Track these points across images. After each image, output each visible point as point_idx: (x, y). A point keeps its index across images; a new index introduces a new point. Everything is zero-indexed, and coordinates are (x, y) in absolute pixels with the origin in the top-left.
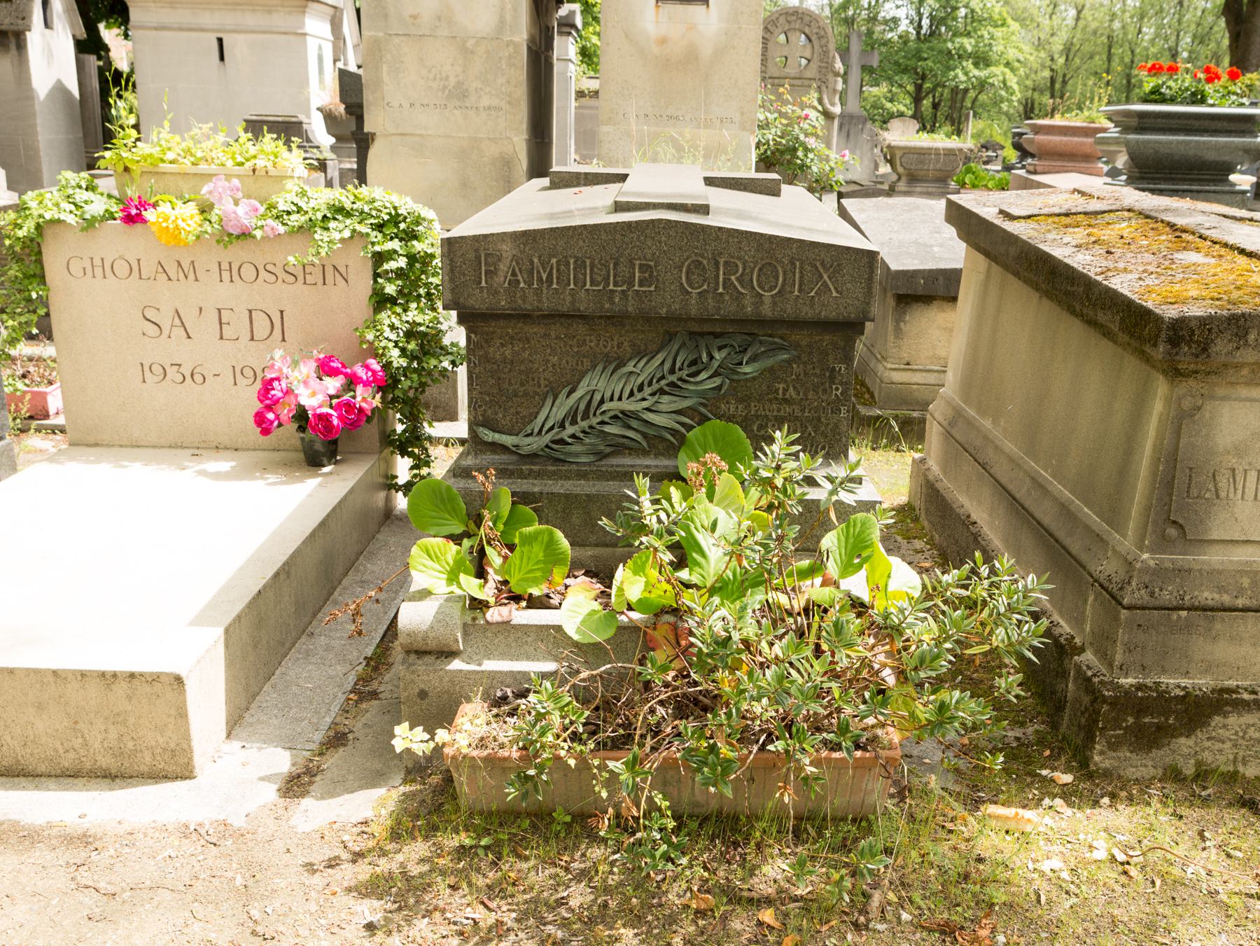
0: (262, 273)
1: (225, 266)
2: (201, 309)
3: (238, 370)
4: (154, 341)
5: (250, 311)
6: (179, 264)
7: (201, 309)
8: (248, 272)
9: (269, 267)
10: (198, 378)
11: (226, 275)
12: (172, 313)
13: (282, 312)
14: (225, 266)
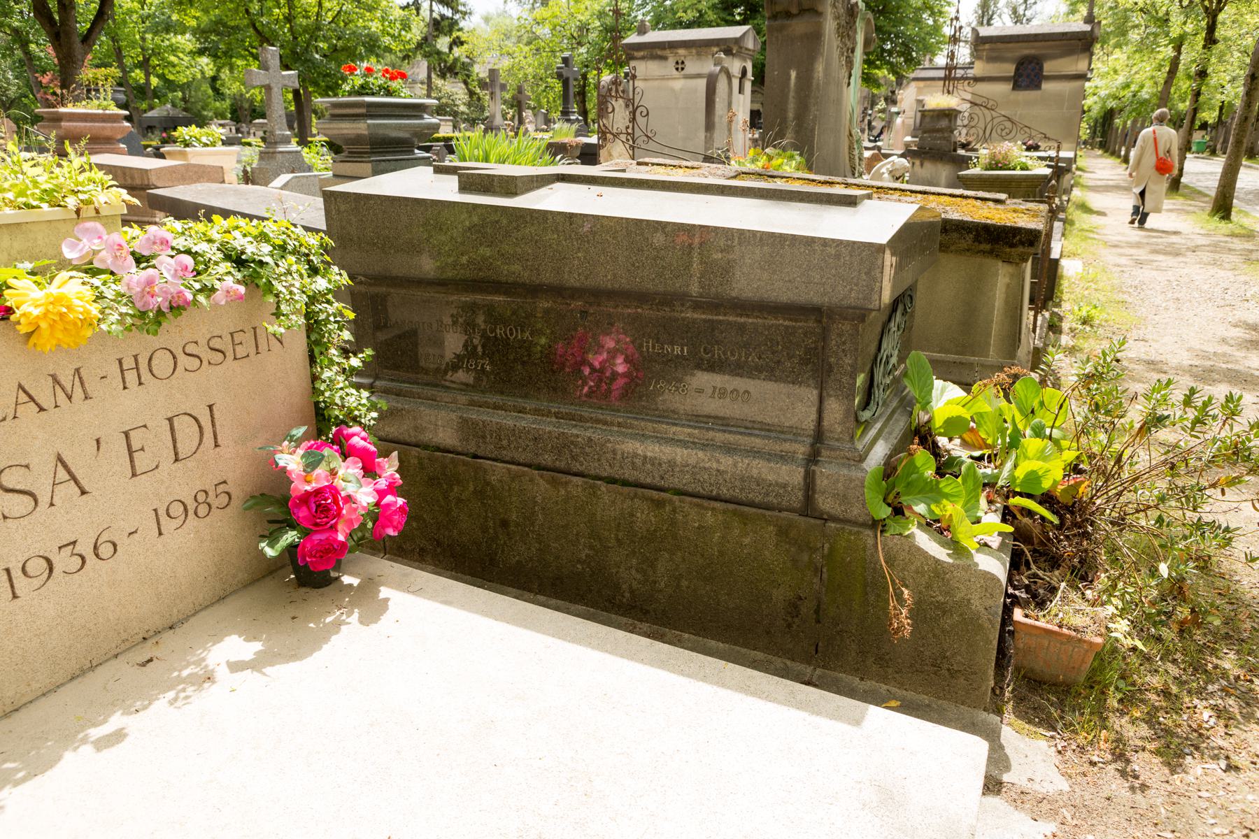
0: (182, 359)
1: (129, 363)
2: (98, 441)
3: (162, 512)
4: (24, 522)
5: (170, 420)
6: (54, 377)
7: (98, 441)
8: (162, 363)
9: (189, 349)
10: (106, 550)
11: (131, 377)
12: (53, 459)
13: (210, 407)
14: (129, 363)
